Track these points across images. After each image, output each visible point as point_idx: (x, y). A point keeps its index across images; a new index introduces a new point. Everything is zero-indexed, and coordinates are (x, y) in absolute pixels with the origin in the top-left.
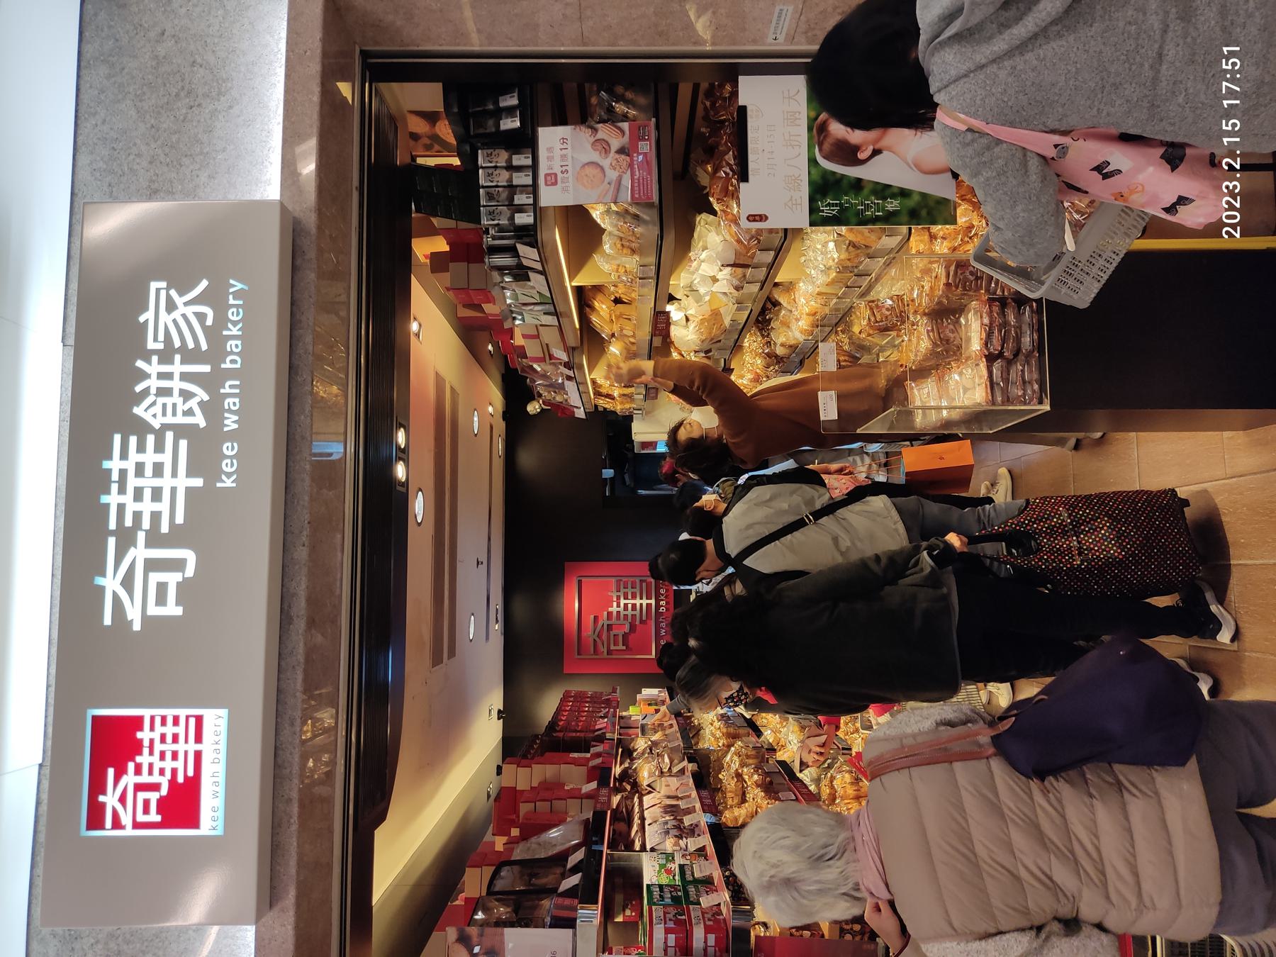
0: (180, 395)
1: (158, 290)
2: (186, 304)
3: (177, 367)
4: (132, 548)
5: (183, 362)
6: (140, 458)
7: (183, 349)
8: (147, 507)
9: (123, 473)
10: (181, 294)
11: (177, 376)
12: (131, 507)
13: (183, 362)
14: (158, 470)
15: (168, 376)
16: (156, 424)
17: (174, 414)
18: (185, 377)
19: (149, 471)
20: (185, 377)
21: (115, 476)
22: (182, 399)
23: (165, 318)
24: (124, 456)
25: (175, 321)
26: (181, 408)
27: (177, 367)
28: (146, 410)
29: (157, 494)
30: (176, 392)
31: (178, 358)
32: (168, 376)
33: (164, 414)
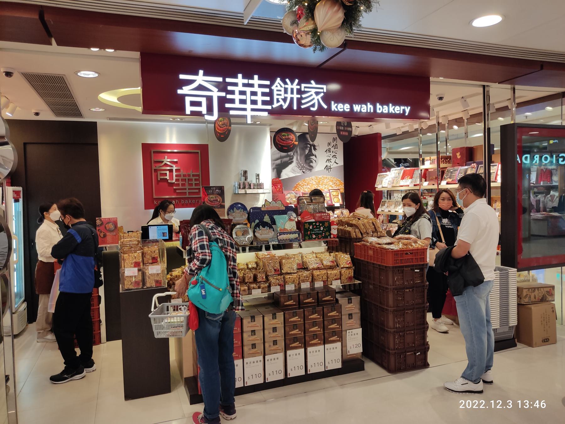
0: (285, 97)
1: (322, 88)
2: (318, 100)
3: (296, 96)
4: (217, 90)
5: (297, 98)
7: (302, 98)
10: (323, 98)
11: (292, 96)
13: (297, 98)
15: (292, 92)
16: (273, 87)
17: (278, 95)
18: (292, 99)
20: (292, 99)
22: (283, 98)
23: (314, 91)
25: (312, 95)
26: (280, 98)
27: (296, 96)
28: (279, 83)
30: (286, 95)
31: (299, 96)
32: (292, 92)
33: (277, 90)
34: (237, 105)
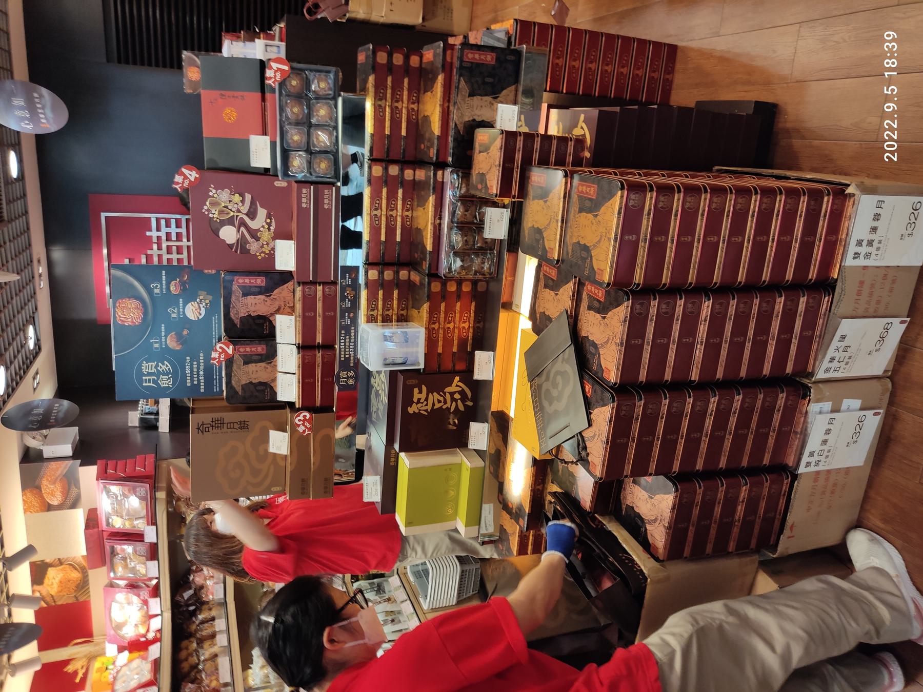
6: (168, 230)
8: (175, 256)
9: (159, 238)
12: (165, 257)
14: (179, 237)
19: (174, 238)
21: (155, 240)
24: (158, 229)
29: (179, 250)
34: (185, 255)
